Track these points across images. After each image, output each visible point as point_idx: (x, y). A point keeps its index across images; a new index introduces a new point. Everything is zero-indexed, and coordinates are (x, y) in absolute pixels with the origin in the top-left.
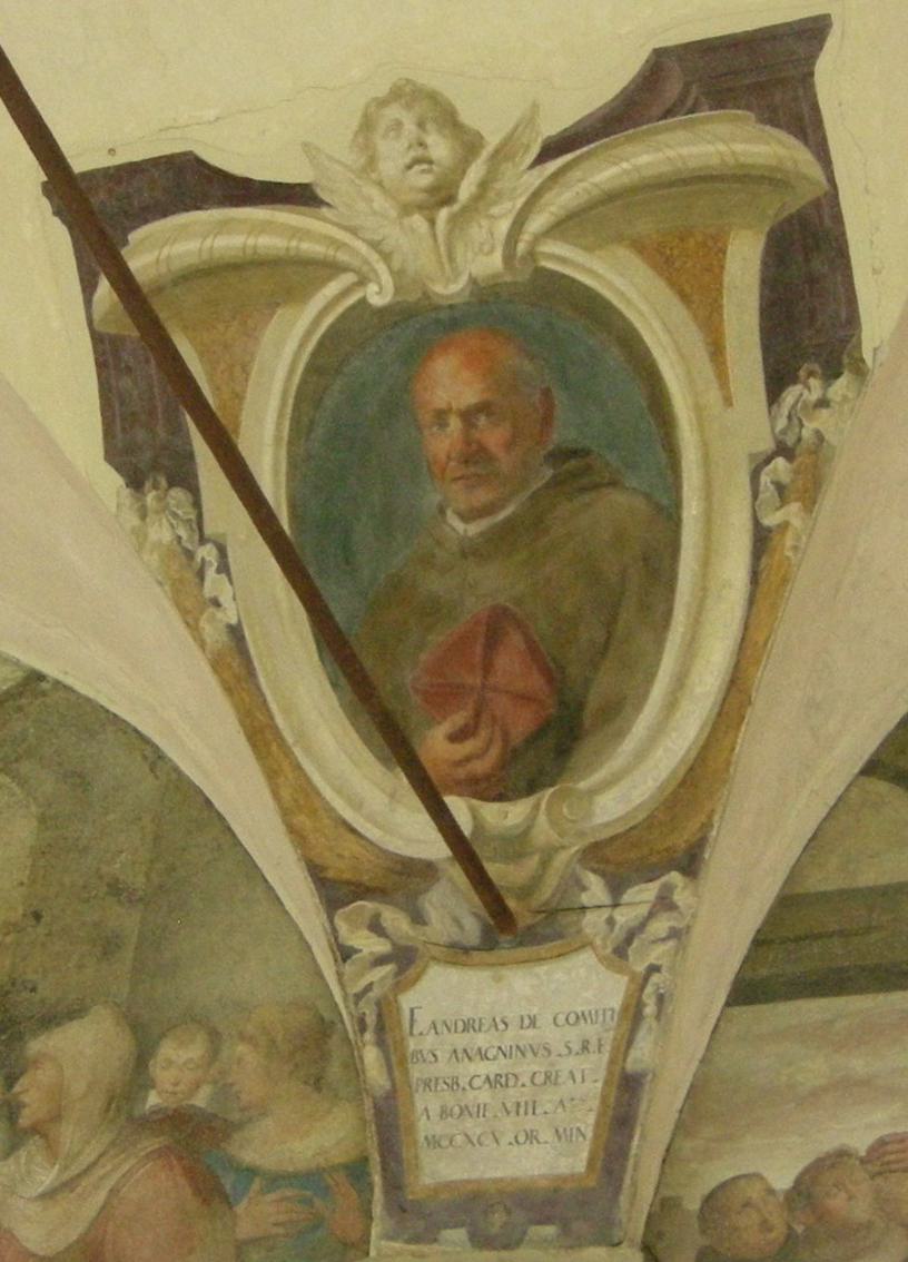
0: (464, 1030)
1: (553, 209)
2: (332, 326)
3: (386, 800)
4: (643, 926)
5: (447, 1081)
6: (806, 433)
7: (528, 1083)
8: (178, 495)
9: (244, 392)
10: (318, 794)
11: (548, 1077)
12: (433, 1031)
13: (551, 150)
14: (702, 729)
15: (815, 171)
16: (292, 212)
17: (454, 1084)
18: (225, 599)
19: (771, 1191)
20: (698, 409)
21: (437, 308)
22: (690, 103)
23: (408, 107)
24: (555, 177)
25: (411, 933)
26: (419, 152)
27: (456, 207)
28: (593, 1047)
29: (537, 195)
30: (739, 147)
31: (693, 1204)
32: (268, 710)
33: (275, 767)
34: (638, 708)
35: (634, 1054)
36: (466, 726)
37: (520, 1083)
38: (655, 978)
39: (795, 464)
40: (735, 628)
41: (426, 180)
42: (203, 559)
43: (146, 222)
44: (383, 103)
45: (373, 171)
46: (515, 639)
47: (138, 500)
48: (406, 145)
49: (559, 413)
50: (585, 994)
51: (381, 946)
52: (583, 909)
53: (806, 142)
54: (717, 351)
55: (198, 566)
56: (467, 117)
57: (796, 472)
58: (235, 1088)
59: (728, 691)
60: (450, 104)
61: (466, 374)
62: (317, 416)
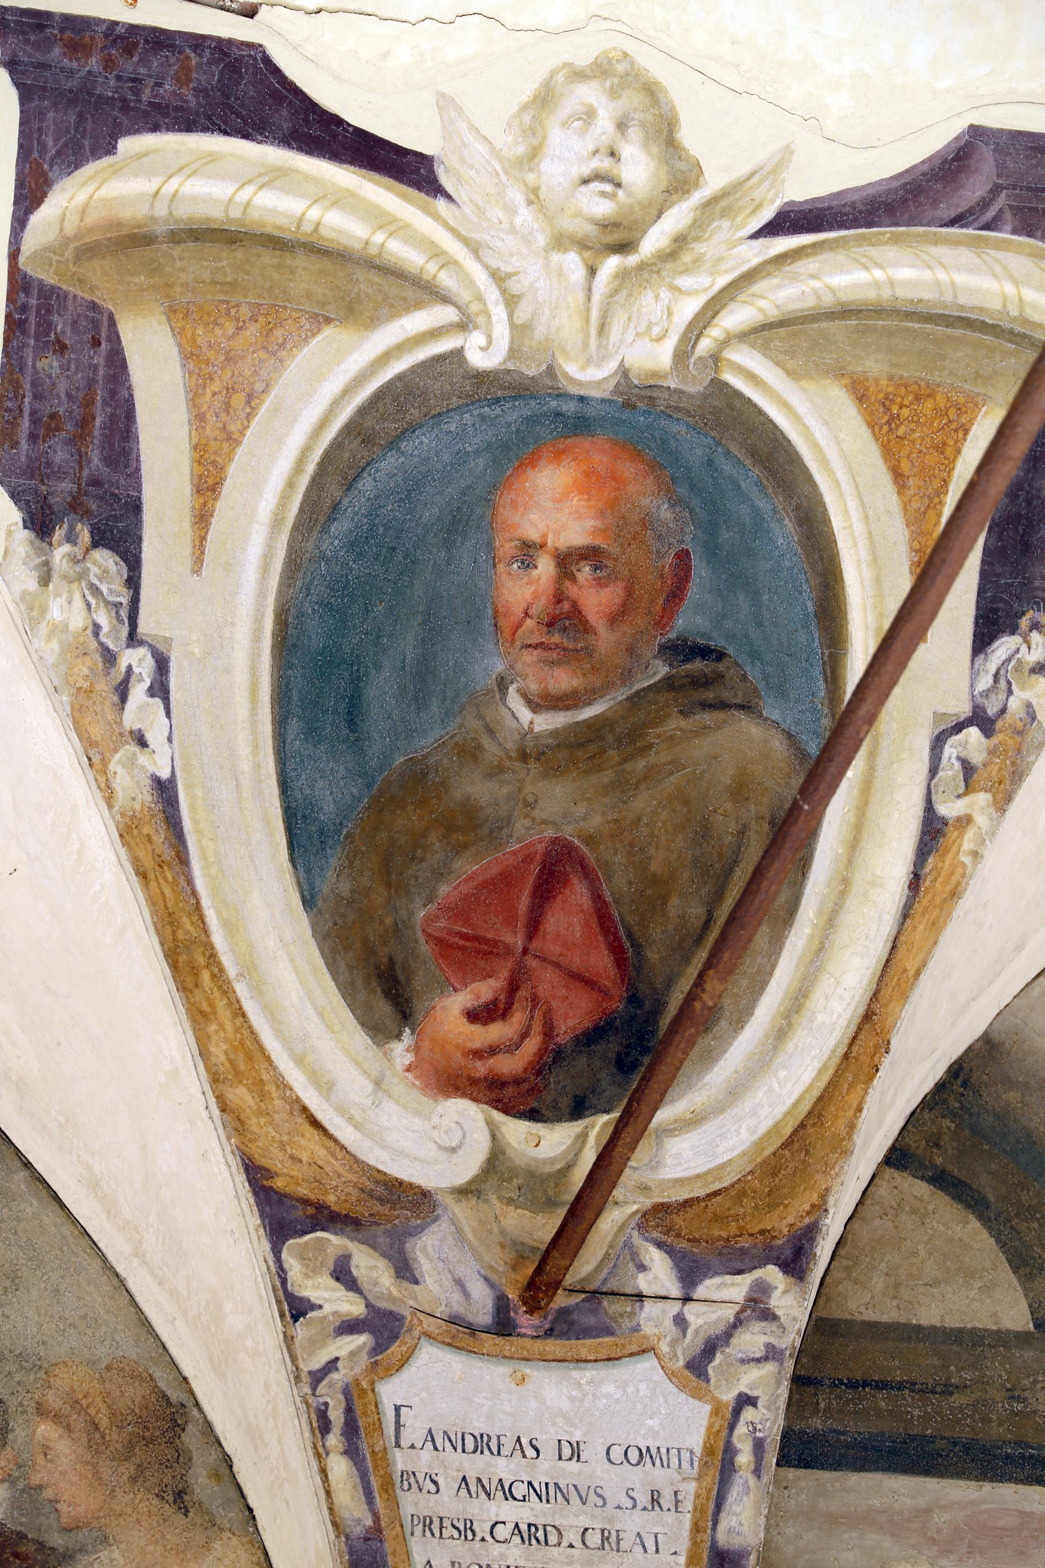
0: (475, 1451)
1: (763, 304)
2: (400, 377)
3: (370, 1087)
4: (727, 1335)
5: (455, 1523)
6: (1015, 704)
7: (578, 1544)
8: (105, 560)
9: (242, 433)
10: (268, 1059)
11: (605, 1538)
12: (429, 1445)
14: (820, 1072)
16: (390, 189)
17: (467, 1530)
18: (156, 737)
21: (561, 395)
22: (990, 214)
23: (613, 93)
25: (395, 1292)
26: (603, 163)
27: (632, 260)
28: (667, 1501)
29: (750, 277)
32: (202, 919)
33: (205, 1007)
35: (726, 1522)
36: (495, 1001)
37: (565, 1543)
38: (748, 1414)
39: (995, 740)
40: (878, 947)
41: (603, 208)
42: (129, 668)
43: (155, 129)
44: (578, 75)
45: (531, 170)
46: (578, 893)
47: (40, 552)
48: (591, 147)
49: (694, 592)
50: (650, 1422)
51: (352, 1306)
52: (640, 1297)
55: (120, 678)
56: (687, 136)
57: (992, 752)
58: (48, 1494)
60: (673, 109)
61: (576, 501)
62: (346, 501)
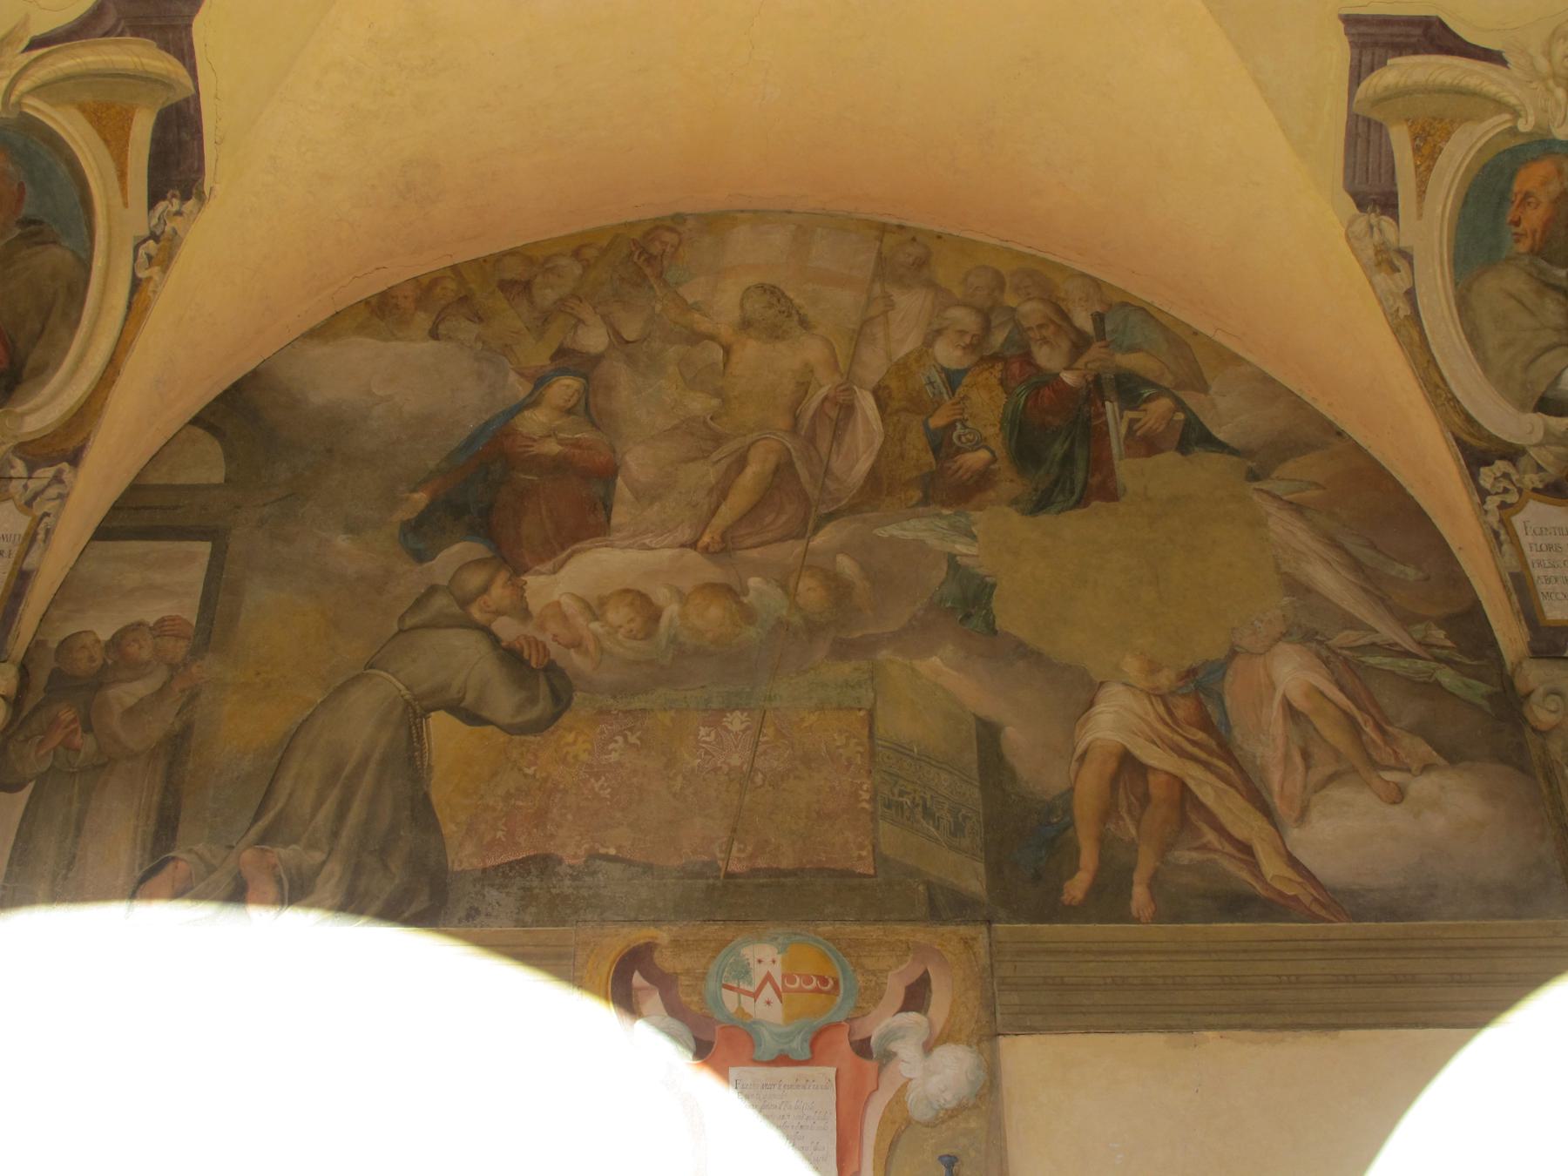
1: (33, 78)
4: (43, 491)
6: (168, 229)
13: (36, 43)
14: (90, 385)
15: (188, 82)
19: (98, 641)
20: (109, 207)
22: (119, 30)
24: (36, 60)
29: (25, 69)
30: (145, 61)
31: (53, 645)
34: (56, 369)
35: (28, 560)
38: (46, 520)
39: (161, 244)
40: (115, 333)
52: (11, 478)
53: (184, 64)
54: (122, 175)
57: (159, 250)
59: (107, 366)
